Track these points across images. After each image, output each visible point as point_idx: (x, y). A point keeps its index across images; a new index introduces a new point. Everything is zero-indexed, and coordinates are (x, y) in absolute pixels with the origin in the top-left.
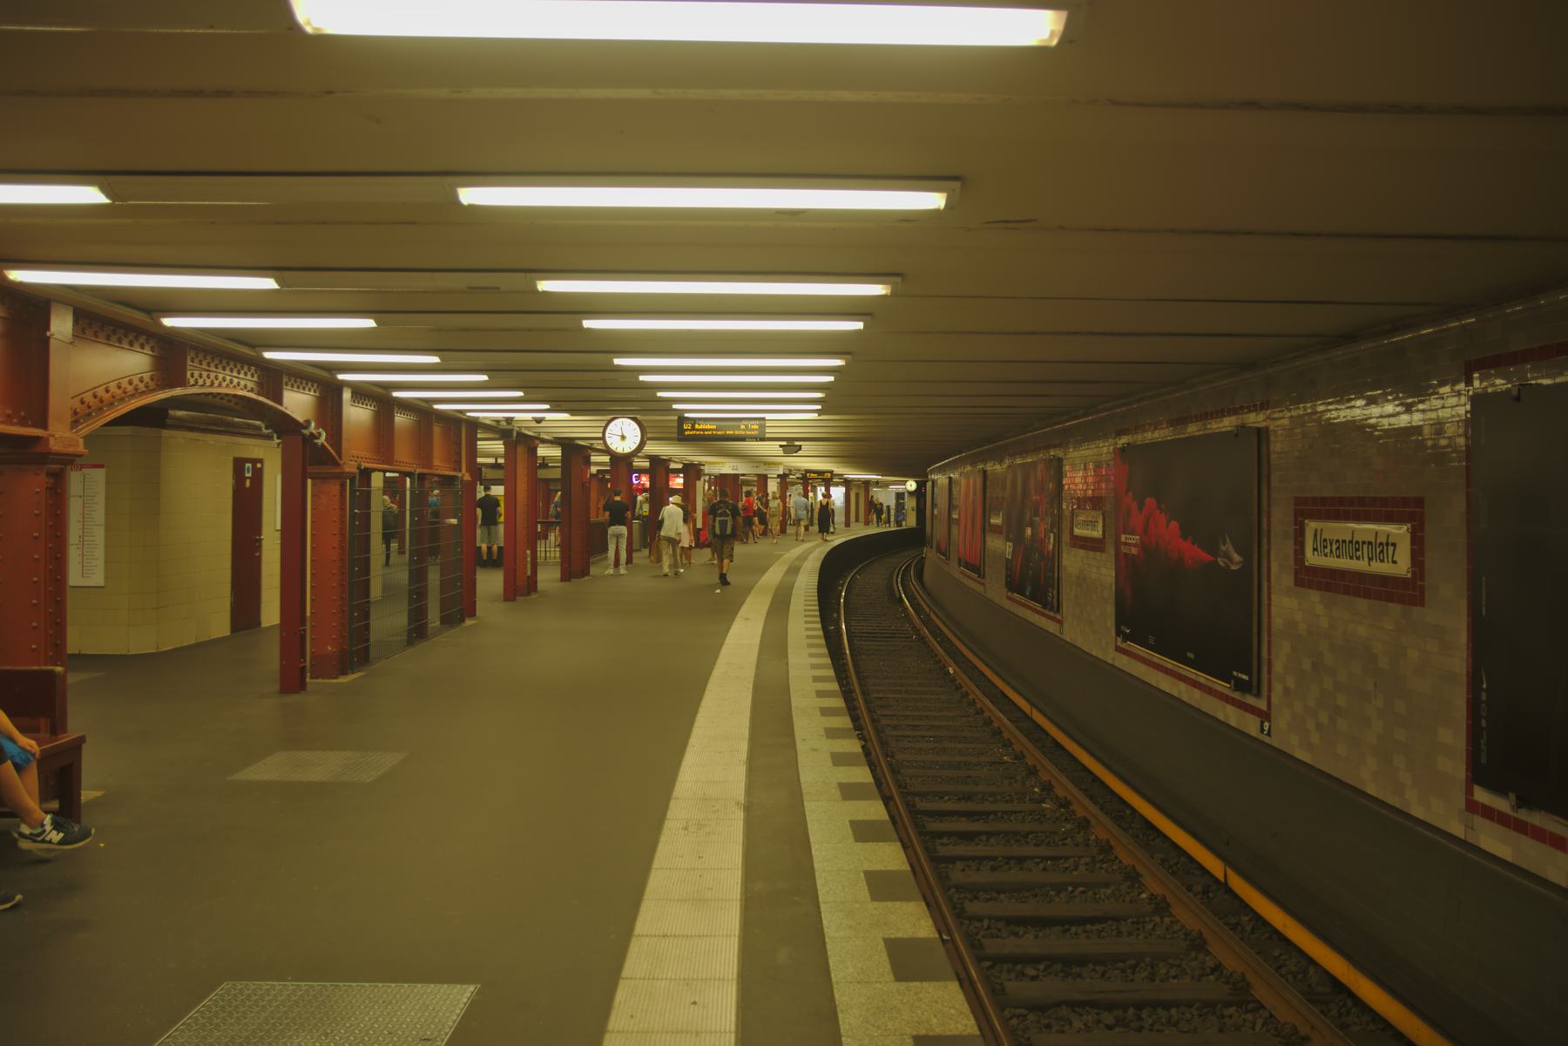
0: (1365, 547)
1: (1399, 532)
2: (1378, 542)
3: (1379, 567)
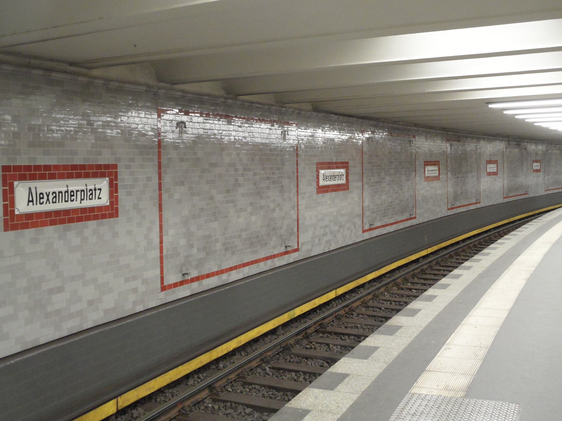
0: (79, 193)
1: (103, 184)
3: (95, 203)
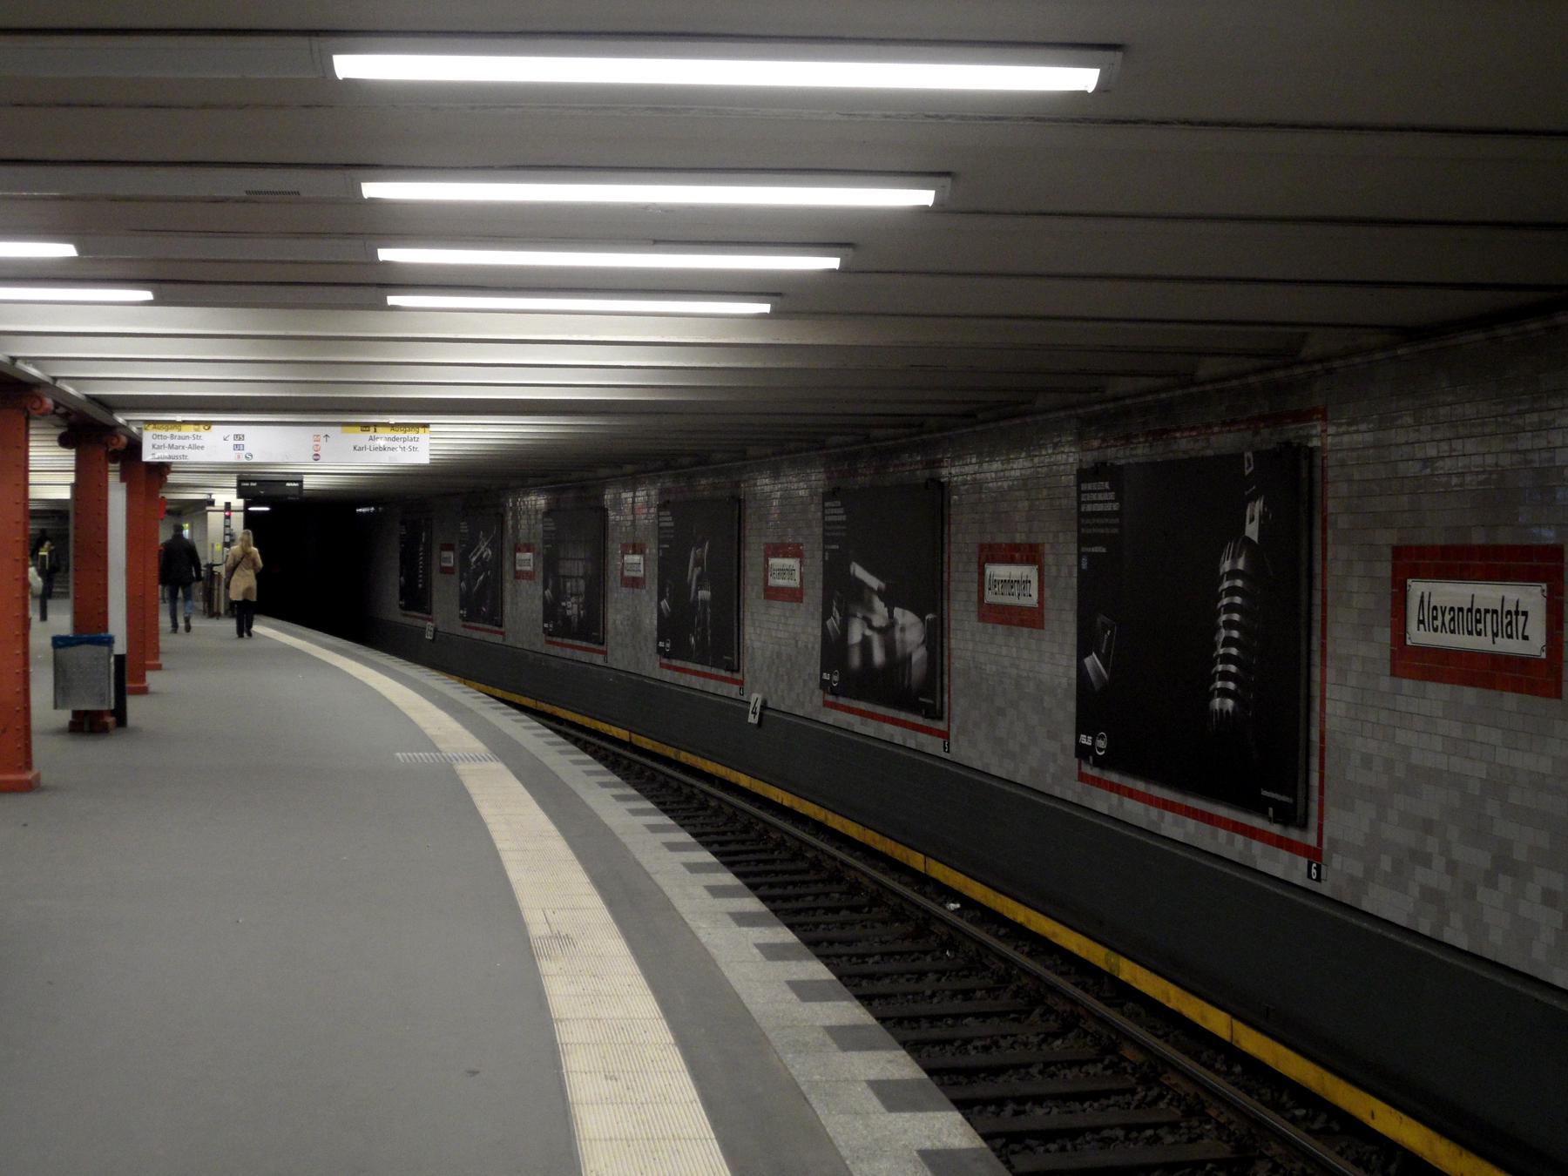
2: (1505, 610)
